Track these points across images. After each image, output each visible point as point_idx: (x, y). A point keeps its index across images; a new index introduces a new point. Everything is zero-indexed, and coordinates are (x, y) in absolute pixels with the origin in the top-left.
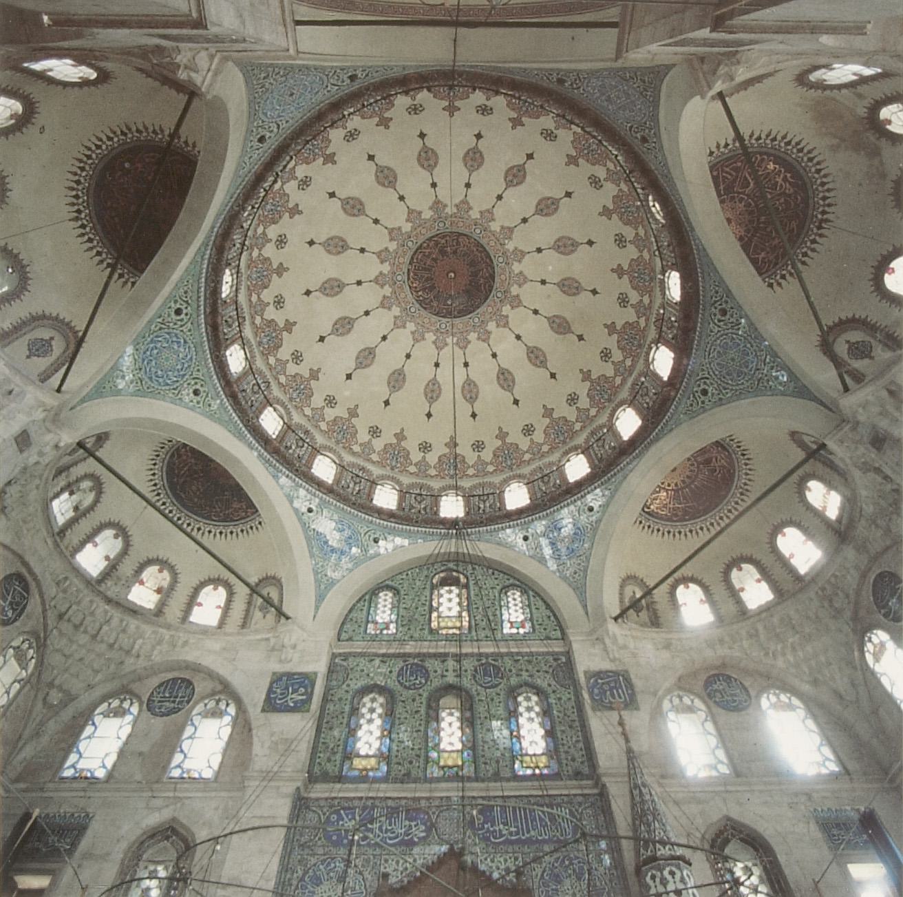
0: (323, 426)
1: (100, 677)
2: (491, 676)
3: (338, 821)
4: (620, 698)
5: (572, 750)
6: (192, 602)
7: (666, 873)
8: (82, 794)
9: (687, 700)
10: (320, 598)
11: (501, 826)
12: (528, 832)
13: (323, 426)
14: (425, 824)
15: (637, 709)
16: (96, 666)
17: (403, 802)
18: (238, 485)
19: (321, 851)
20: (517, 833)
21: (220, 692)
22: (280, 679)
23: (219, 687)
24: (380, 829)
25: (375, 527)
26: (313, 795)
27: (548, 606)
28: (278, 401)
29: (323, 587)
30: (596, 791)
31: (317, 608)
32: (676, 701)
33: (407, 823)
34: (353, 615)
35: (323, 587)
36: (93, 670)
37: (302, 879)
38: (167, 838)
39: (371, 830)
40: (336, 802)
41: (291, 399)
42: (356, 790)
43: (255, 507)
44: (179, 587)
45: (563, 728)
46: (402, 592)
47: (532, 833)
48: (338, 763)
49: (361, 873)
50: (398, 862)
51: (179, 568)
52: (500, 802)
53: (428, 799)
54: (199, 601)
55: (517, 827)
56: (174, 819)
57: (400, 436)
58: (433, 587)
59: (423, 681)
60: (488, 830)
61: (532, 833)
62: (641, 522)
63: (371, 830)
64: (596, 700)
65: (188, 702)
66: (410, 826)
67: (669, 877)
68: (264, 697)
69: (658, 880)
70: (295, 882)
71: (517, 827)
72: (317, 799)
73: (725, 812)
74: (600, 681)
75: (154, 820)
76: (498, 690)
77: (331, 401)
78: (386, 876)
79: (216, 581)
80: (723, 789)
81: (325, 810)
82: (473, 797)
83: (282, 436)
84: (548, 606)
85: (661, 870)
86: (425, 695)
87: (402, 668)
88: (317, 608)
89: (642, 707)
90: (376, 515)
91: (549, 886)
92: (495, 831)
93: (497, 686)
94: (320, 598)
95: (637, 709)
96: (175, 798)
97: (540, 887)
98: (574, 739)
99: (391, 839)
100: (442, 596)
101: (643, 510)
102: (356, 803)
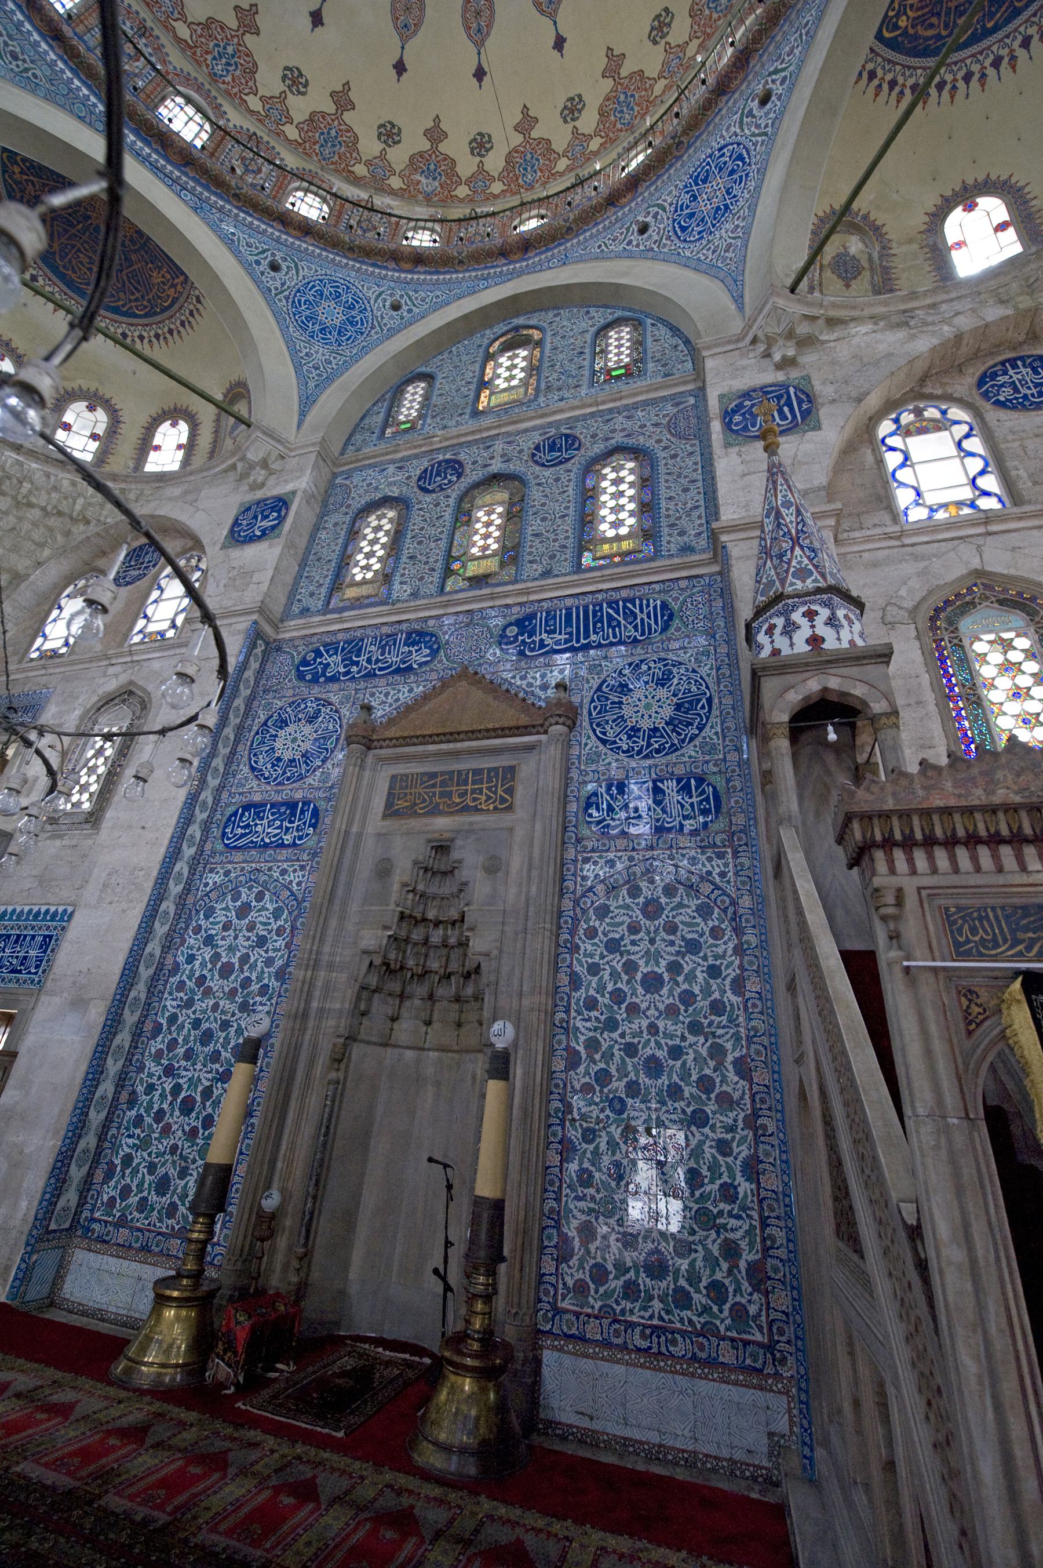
0: (292, 132)
1: (47, 552)
2: (560, 450)
3: (315, 660)
4: (783, 417)
5: (684, 522)
6: (145, 445)
7: (797, 616)
8: (43, 672)
9: (932, 413)
10: (307, 403)
11: (544, 636)
12: (587, 636)
13: (292, 132)
14: (430, 648)
15: (818, 427)
16: (36, 536)
17: (404, 626)
18: (139, 232)
19: (291, 692)
20: (566, 641)
21: (191, 549)
22: (248, 509)
23: (190, 543)
24: (369, 661)
25: (392, 284)
26: (287, 635)
27: (675, 331)
28: (187, 80)
29: (311, 384)
30: (715, 568)
31: (303, 414)
32: (907, 418)
33: (406, 649)
34: (367, 421)
35: (311, 384)
36: (35, 543)
37: (265, 724)
38: (124, 701)
39: (357, 663)
40: (315, 639)
41: (214, 77)
42: (341, 621)
43: (183, 273)
44: (124, 429)
45: (672, 494)
46: (440, 376)
47: (593, 637)
48: (322, 596)
49: (336, 711)
50: (387, 695)
51: (118, 402)
52: (545, 605)
53: (438, 617)
54: (155, 442)
55: (571, 634)
56: (131, 683)
57: (436, 134)
58: (489, 357)
59: (455, 479)
60: (523, 641)
61: (593, 637)
62: (872, 75)
63: (357, 663)
64: (736, 432)
65: (154, 566)
66: (410, 652)
67: (804, 622)
68: (225, 533)
69: (777, 631)
70: (255, 728)
71: (571, 634)
72: (292, 640)
73: (976, 563)
74: (747, 403)
75: (112, 685)
76: (568, 465)
77: (295, 80)
78: (368, 708)
79: (174, 414)
80: (981, 530)
81: (300, 649)
82: (507, 606)
83: (212, 149)
84: (675, 331)
85: (786, 613)
86: (454, 495)
87: (426, 471)
88: (303, 414)
89: (825, 423)
90: (393, 265)
91: (607, 699)
92: (534, 642)
93: (567, 460)
94: (307, 403)
95: (818, 427)
96: (132, 662)
97: (593, 701)
98: (689, 505)
99: (380, 669)
100: (501, 365)
101: (879, 37)
102: (340, 636)
